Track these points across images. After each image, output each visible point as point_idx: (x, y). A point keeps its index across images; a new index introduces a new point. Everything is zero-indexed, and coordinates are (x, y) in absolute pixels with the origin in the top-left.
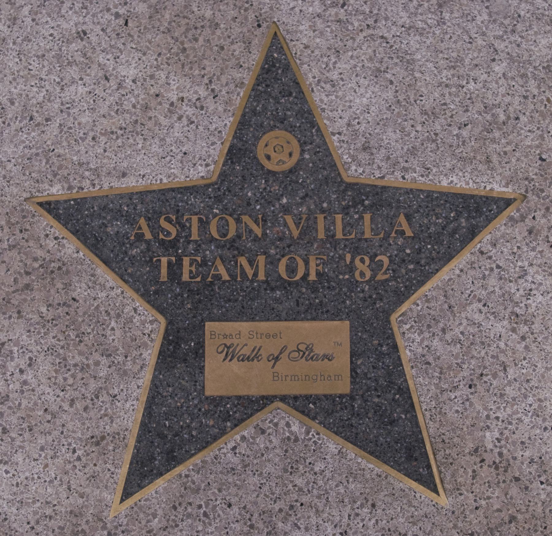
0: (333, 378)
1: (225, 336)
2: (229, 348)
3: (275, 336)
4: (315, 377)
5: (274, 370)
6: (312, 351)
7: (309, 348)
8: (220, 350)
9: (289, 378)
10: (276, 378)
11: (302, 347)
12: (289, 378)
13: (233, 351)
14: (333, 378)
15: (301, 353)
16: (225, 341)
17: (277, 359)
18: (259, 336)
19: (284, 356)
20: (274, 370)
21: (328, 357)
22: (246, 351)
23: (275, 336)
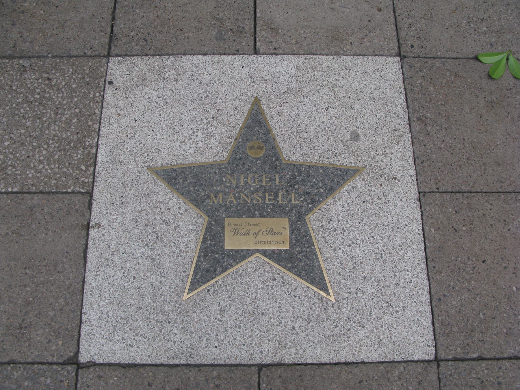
0: (281, 242)
1: (235, 225)
2: (236, 230)
3: (257, 225)
4: (273, 242)
5: (256, 239)
6: (272, 231)
7: (271, 229)
8: (232, 230)
9: (262, 243)
10: (256, 243)
11: (268, 230)
12: (262, 243)
13: (238, 231)
14: (281, 242)
15: (268, 232)
16: (235, 227)
17: (257, 234)
18: (250, 225)
19: (260, 233)
20: (256, 239)
21: (281, 234)
22: (244, 231)
23: (257, 225)
